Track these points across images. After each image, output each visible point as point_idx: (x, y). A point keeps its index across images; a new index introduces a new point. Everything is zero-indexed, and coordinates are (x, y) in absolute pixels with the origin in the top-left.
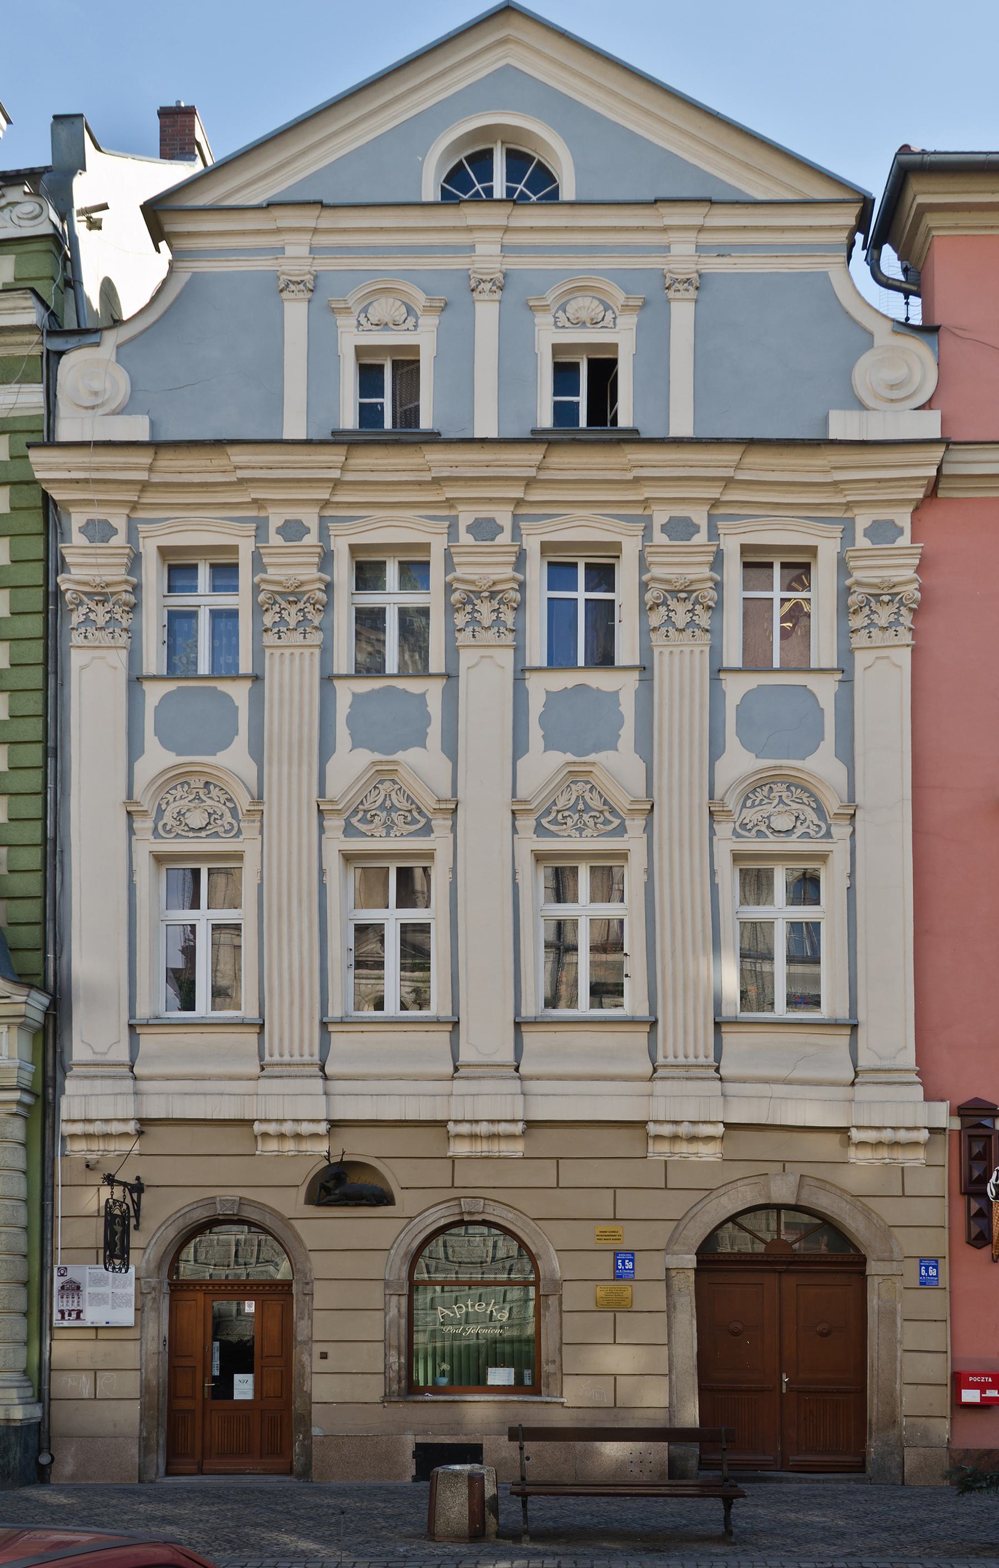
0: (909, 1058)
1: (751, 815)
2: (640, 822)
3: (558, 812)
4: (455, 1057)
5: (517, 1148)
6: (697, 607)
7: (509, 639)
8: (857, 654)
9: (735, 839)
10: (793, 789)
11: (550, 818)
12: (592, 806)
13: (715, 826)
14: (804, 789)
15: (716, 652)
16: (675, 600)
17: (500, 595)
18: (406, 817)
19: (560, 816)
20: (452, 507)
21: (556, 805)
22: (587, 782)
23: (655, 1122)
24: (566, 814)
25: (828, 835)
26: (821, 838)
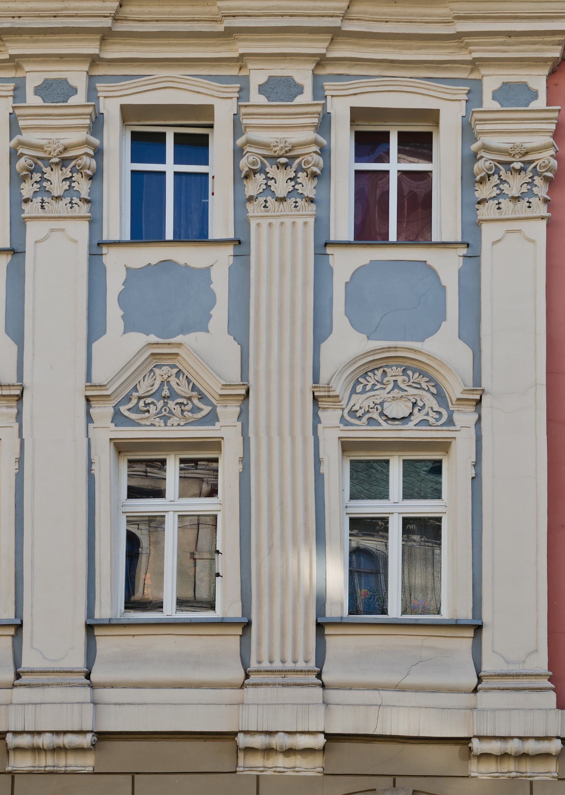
0: (540, 662)
1: (360, 402)
2: (233, 409)
3: (140, 398)
4: (17, 662)
5: (87, 762)
6: (300, 174)
7: (84, 210)
8: (485, 227)
9: (342, 427)
10: (410, 373)
11: (131, 405)
12: (179, 392)
13: (320, 413)
14: (422, 373)
15: (321, 224)
16: (275, 167)
17: (73, 163)
19: (141, 403)
20: (18, 67)
21: (137, 391)
22: (173, 366)
23: (246, 732)
24: (149, 400)
25: (450, 422)
26: (441, 425)
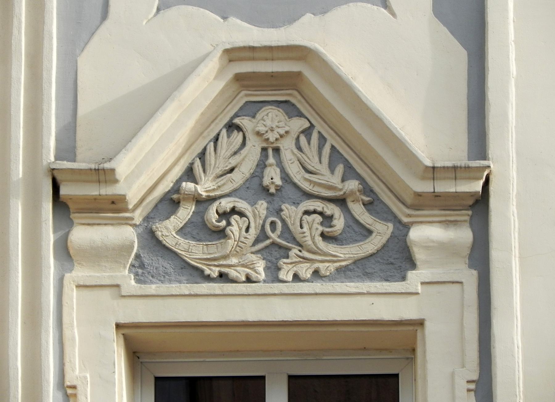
18: (328, 219)
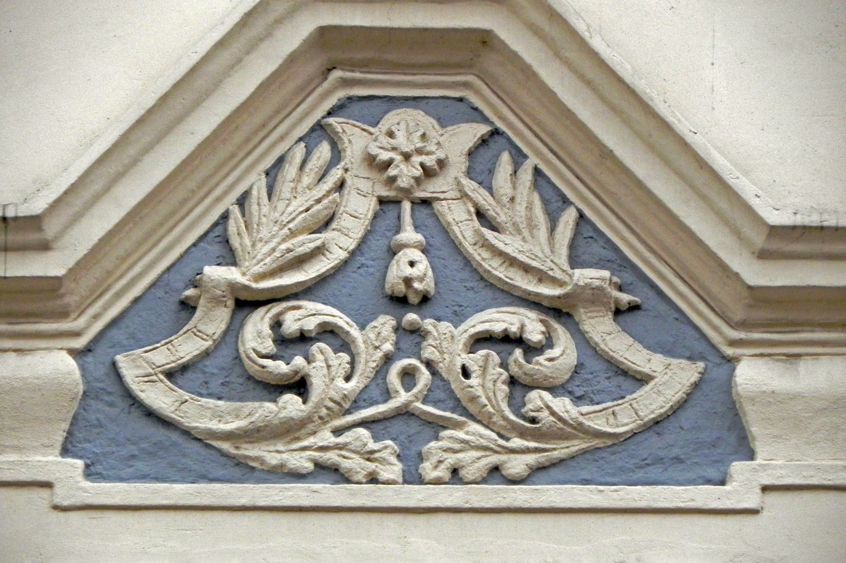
3: (245, 303)
11: (187, 347)
